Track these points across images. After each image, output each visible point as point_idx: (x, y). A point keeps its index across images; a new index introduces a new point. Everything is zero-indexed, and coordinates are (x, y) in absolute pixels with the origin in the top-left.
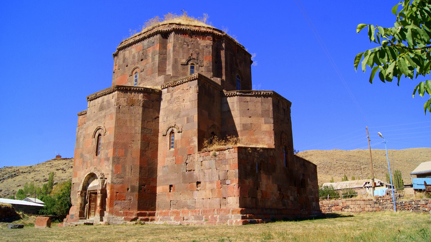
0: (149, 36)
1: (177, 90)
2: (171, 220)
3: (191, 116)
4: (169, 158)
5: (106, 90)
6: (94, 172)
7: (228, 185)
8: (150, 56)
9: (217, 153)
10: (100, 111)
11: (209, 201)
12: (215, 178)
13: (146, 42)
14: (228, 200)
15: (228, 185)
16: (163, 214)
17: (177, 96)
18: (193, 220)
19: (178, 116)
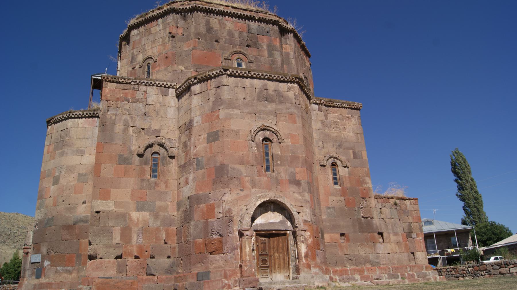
0: (260, 20)
1: (334, 113)
2: (357, 280)
3: (359, 151)
4: (334, 197)
5: (277, 74)
6: (279, 200)
7: (414, 238)
8: (265, 47)
9: (398, 202)
10: (258, 100)
11: (396, 256)
12: (399, 229)
13: (254, 25)
14: (417, 255)
15: (414, 238)
16: (338, 272)
17: (334, 121)
18: (386, 279)
19: (340, 146)
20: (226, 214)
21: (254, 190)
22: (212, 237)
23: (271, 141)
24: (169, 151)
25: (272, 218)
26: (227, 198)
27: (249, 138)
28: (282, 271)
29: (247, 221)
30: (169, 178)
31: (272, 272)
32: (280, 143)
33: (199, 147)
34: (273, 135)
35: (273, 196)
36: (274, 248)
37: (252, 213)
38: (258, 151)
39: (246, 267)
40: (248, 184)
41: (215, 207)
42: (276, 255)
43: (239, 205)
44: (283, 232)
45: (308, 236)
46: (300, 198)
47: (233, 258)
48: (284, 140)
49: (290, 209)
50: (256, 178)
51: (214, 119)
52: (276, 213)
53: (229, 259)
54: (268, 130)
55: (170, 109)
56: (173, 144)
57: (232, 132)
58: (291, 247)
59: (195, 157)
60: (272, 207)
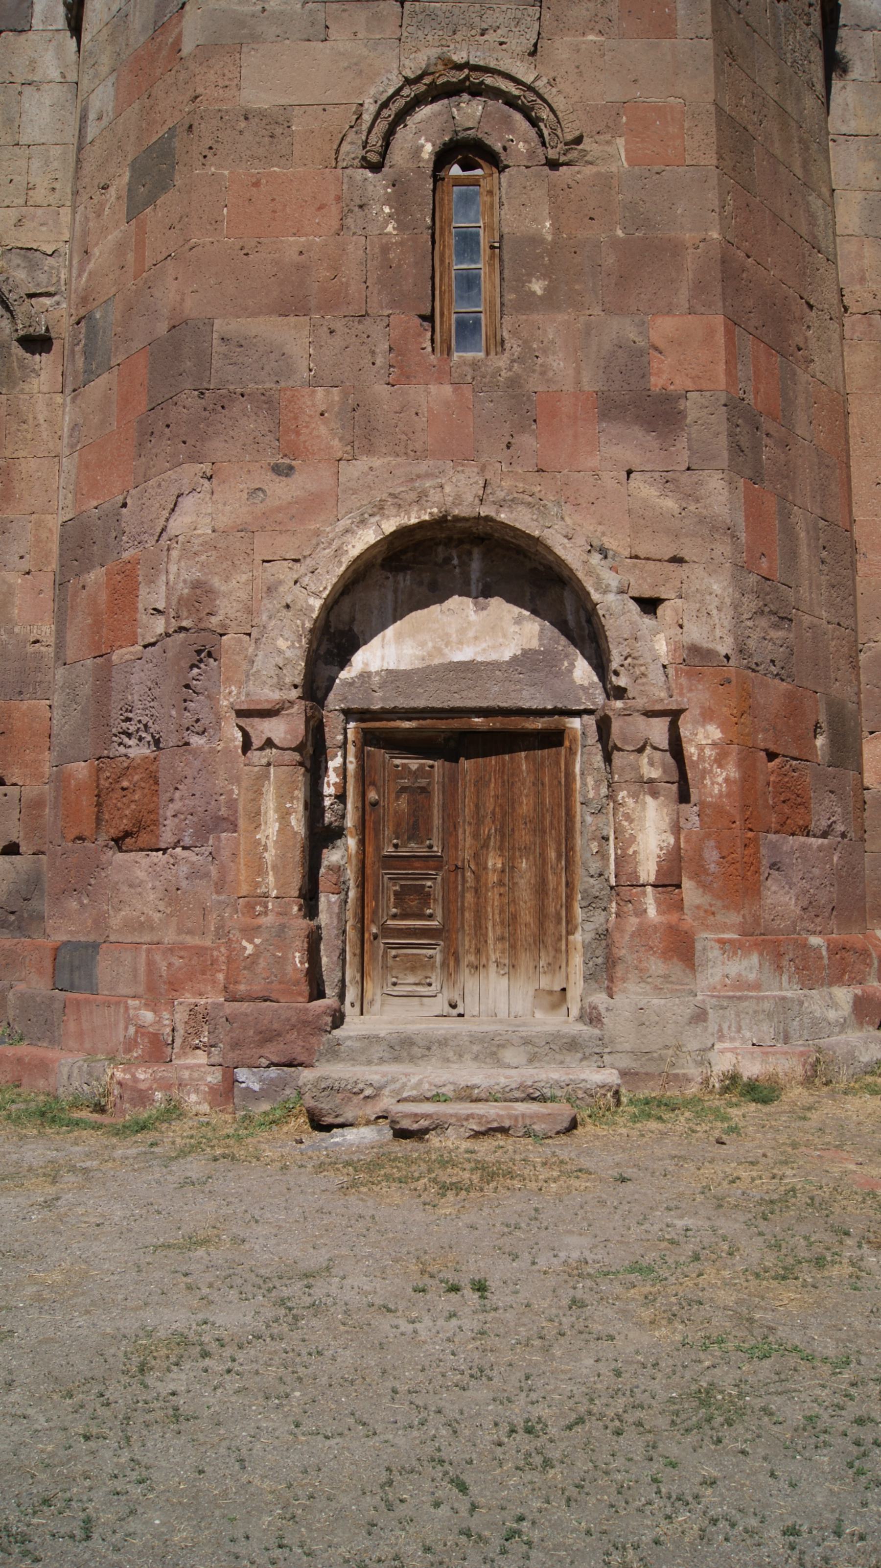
6: (503, 517)
20: (177, 617)
21: (363, 464)
22: (122, 749)
23: (494, 160)
24: (19, 310)
25: (471, 634)
26: (188, 519)
27: (351, 149)
28: (525, 959)
29: (280, 652)
30: (21, 454)
31: (457, 961)
32: (553, 165)
33: (96, 251)
34: (507, 121)
35: (469, 498)
36: (479, 821)
37: (317, 604)
38: (401, 227)
39: (251, 941)
40: (323, 430)
41: (140, 579)
42: (494, 861)
43: (258, 558)
44: (539, 724)
45: (708, 752)
46: (670, 504)
47: (207, 875)
48: (578, 140)
49: (580, 575)
50: (381, 389)
51: (158, 71)
52: (496, 603)
53: (184, 884)
54: (476, 91)
55: (37, 95)
56: (43, 278)
57: (243, 124)
58: (589, 819)
59: (82, 312)
60: (476, 566)
